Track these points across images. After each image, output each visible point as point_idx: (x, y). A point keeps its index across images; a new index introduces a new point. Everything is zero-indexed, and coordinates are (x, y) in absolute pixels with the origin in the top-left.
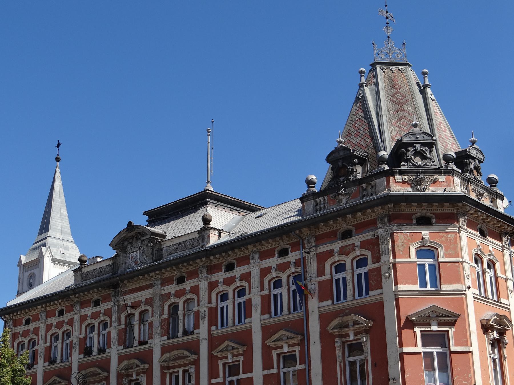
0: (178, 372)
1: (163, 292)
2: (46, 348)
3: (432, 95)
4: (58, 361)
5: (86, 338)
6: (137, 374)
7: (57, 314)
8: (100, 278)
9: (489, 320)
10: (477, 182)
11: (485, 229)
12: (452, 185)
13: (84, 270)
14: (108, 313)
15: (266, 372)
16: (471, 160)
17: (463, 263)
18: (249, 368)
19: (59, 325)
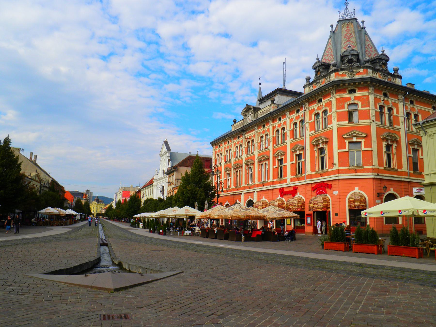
1: (259, 132)
5: (236, 152)
15: (291, 163)
18: (286, 162)
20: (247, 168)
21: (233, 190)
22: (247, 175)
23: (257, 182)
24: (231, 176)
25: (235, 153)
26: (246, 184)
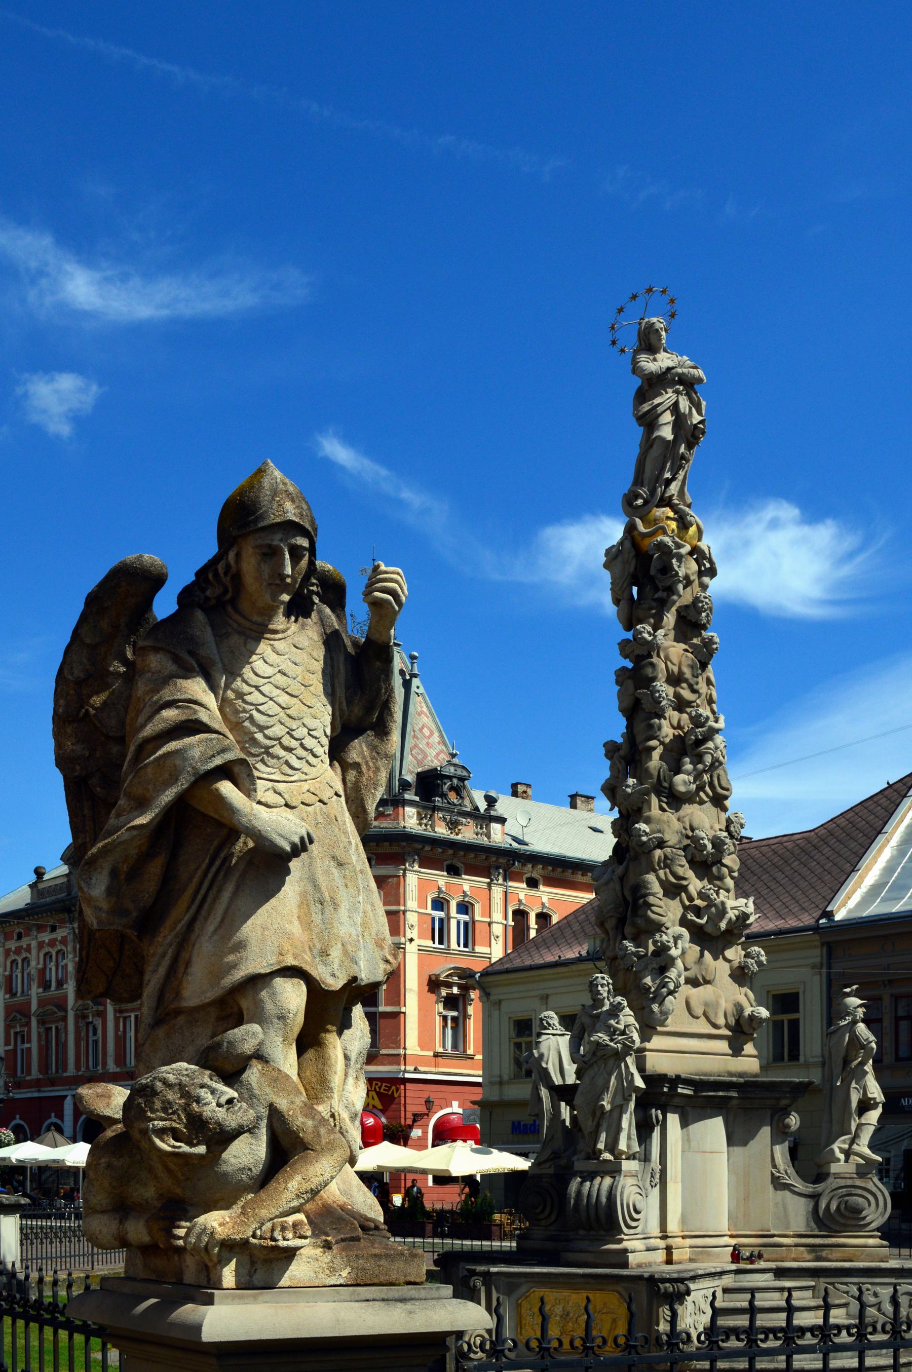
0: (130, 1017)
2: (6, 977)
3: (418, 687)
4: (19, 995)
6: (93, 1016)
7: (15, 937)
8: (53, 898)
9: (438, 976)
10: (449, 808)
11: (459, 865)
12: (401, 817)
13: (41, 886)
14: (64, 941)
16: (446, 781)
17: (404, 912)
19: (18, 951)
20: (82, 1024)
21: (38, 1084)
22: (83, 1044)
23: (112, 1067)
24: (29, 1041)
25: (42, 972)
26: (78, 1068)
